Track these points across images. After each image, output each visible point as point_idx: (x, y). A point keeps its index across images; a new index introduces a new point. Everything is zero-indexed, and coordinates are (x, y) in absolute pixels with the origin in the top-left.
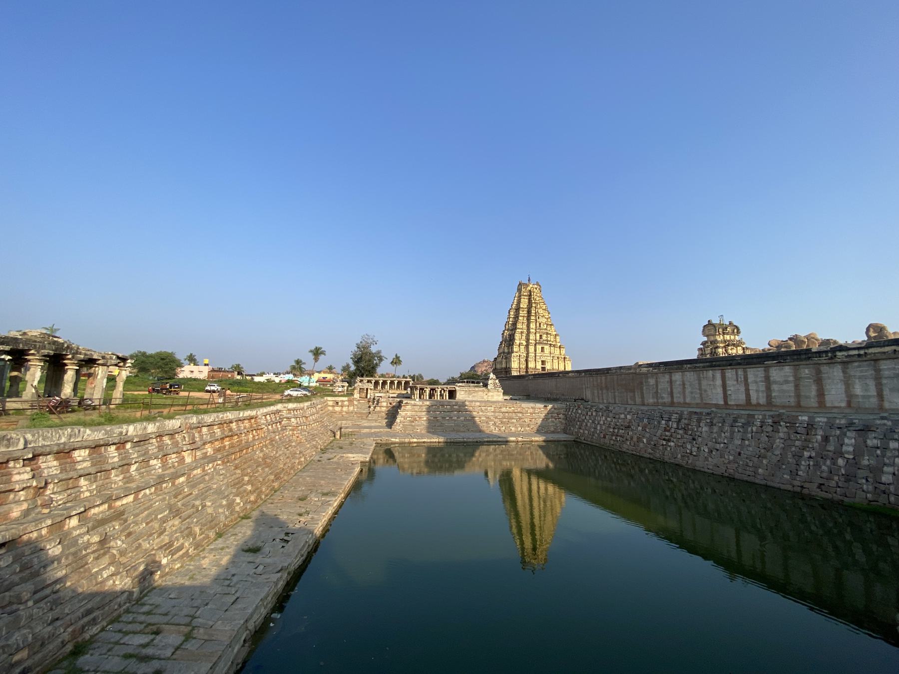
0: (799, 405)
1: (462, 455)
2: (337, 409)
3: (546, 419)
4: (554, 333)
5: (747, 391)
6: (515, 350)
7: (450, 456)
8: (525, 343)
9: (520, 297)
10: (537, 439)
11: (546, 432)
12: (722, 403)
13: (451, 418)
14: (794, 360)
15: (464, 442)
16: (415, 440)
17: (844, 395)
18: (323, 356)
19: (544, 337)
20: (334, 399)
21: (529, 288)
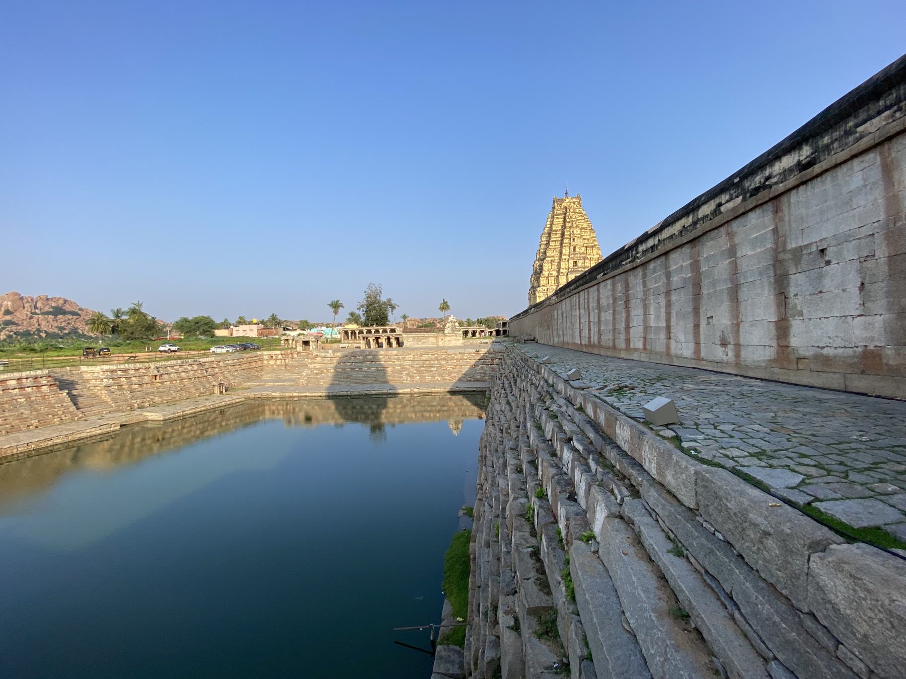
0: (614, 347)
1: (374, 407)
2: (272, 362)
4: (596, 257)
5: (590, 322)
7: (362, 408)
8: (555, 273)
9: (553, 217)
11: (470, 381)
13: (361, 369)
14: (614, 268)
16: (296, 394)
17: (642, 327)
19: (579, 264)
20: (268, 353)
21: (564, 204)
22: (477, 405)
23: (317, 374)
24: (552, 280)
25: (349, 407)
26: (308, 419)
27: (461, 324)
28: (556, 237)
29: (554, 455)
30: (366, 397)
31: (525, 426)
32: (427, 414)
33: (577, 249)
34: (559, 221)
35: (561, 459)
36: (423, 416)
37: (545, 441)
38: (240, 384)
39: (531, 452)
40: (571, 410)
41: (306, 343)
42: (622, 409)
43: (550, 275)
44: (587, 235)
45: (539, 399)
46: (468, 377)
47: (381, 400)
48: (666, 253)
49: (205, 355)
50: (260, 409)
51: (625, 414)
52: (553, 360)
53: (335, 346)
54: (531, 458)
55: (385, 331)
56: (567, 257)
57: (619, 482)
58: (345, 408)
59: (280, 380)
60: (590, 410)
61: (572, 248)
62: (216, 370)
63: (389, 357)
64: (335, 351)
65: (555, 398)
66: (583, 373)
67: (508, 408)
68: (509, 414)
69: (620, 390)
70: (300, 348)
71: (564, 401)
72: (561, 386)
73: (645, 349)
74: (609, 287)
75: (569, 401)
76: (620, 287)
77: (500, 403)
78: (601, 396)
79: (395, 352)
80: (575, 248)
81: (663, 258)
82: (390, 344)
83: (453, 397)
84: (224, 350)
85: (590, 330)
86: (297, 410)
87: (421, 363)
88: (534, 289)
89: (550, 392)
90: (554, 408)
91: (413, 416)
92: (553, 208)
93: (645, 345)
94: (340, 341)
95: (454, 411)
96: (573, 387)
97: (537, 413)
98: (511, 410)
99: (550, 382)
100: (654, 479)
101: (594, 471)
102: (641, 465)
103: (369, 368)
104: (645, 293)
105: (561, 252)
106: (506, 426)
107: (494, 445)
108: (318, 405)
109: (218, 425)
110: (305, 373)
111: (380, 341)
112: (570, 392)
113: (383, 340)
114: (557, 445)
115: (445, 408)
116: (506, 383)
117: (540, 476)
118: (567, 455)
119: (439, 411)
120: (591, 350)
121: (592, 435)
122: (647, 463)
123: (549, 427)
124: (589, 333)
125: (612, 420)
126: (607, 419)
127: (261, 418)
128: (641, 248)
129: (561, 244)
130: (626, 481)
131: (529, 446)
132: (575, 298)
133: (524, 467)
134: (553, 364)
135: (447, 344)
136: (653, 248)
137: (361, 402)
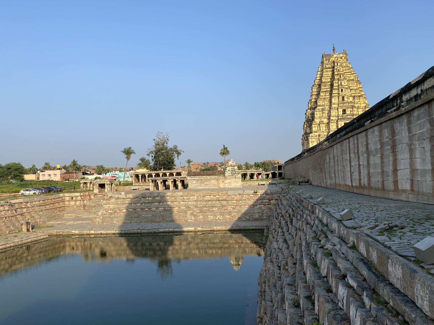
0: (383, 189)
1: (162, 244)
2: (72, 203)
3: (254, 205)
4: (363, 105)
5: (359, 165)
6: (314, 129)
7: (151, 244)
8: (325, 121)
9: (322, 71)
10: (219, 228)
11: (249, 220)
12: (350, 184)
14: (380, 116)
15: (138, 233)
16: (93, 232)
17: (408, 171)
18: (132, 154)
19: (348, 112)
21: (332, 59)
22: (255, 243)
23: (111, 214)
24: (323, 127)
25: (139, 244)
26: (103, 254)
27: (240, 167)
28: (325, 88)
29: (329, 291)
30: (154, 235)
31: (302, 263)
32: (210, 251)
33: (346, 99)
34: (328, 74)
35: (336, 295)
36: (206, 253)
37: (320, 277)
38: (44, 222)
39: (307, 288)
40: (344, 249)
41: (102, 186)
42: (393, 248)
43: (321, 123)
44: (354, 86)
45: (314, 238)
46: (247, 216)
47: (168, 237)
48: (429, 102)
49: (15, 197)
50: (62, 245)
51: (396, 253)
52: (327, 200)
53: (127, 188)
54: (307, 294)
55: (171, 174)
56: (336, 106)
57: (393, 319)
58: (135, 245)
59: (77, 219)
60: (362, 249)
61: (341, 98)
62: (25, 210)
63: (175, 199)
64: (127, 193)
65: (330, 237)
66: (355, 213)
67: (285, 246)
68: (286, 252)
69: (390, 229)
70: (96, 191)
71: (338, 240)
72: (335, 226)
73: (412, 190)
74: (377, 133)
75: (343, 240)
76: (386, 133)
77: (277, 241)
78: (372, 235)
79: (181, 193)
80: (343, 98)
81: (426, 107)
82: (176, 186)
83: (234, 235)
84: (32, 193)
85: (360, 172)
86: (93, 246)
87: (204, 203)
88: (306, 136)
89: (324, 231)
90: (329, 246)
91: (197, 252)
92: (322, 62)
93: (412, 186)
94: (131, 184)
95: (235, 248)
96: (346, 227)
97: (312, 251)
98: (288, 248)
99: (325, 221)
100: (427, 316)
101: (368, 307)
102: (414, 303)
103: (157, 208)
104: (411, 138)
105: (331, 102)
106: (283, 262)
107: (272, 281)
108: (112, 242)
109: (24, 260)
110: (101, 214)
111: (167, 183)
112: (343, 231)
113: (170, 183)
114: (332, 282)
115: (227, 245)
116: (283, 222)
117: (316, 311)
118: (342, 291)
119: (221, 248)
120: (361, 191)
121: (365, 272)
122: (420, 301)
123: (324, 265)
124: (360, 176)
125: (384, 258)
126: (379, 257)
127: (62, 253)
128: (405, 98)
129: (331, 94)
130: (400, 317)
131: (306, 282)
132: (346, 143)
133: (301, 302)
134: (327, 204)
135: (227, 186)
136: (417, 97)
137: (150, 238)
